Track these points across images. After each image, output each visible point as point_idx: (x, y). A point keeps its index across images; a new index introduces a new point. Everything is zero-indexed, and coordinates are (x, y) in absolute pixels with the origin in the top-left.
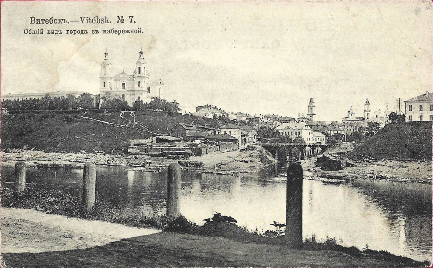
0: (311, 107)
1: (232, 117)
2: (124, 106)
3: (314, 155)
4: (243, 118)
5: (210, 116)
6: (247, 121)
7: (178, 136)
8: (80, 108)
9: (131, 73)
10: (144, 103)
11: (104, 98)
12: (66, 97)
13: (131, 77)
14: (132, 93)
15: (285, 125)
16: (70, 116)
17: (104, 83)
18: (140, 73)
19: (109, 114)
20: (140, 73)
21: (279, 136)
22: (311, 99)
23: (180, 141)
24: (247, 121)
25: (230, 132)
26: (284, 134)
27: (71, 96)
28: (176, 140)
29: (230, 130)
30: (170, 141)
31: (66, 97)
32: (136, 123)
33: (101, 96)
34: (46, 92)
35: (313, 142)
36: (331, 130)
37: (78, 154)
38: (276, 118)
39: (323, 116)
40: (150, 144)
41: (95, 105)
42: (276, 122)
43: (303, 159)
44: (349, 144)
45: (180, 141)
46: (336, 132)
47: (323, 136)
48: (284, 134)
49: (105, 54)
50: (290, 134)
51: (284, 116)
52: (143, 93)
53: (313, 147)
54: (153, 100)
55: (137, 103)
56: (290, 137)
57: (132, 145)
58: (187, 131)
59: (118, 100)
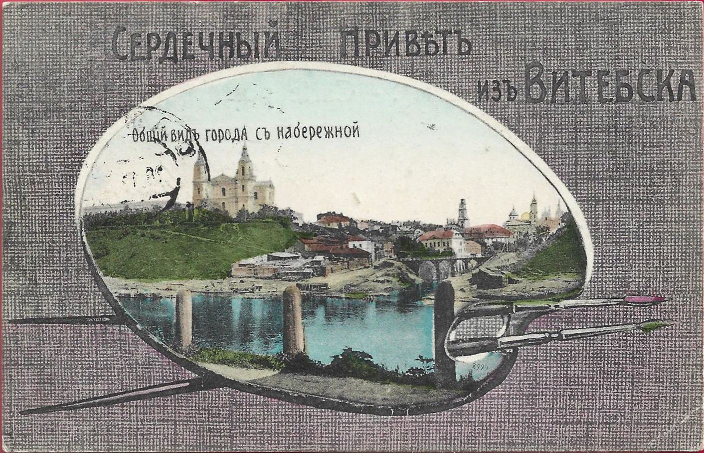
0: (462, 210)
1: (361, 227)
2: (226, 218)
3: (467, 270)
4: (376, 228)
5: (335, 226)
6: (381, 231)
10: (250, 212)
11: (199, 208)
15: (428, 234)
18: (243, 175)
19: (206, 228)
20: (243, 175)
21: (423, 247)
22: (462, 200)
23: (298, 257)
24: (381, 231)
25: (360, 245)
26: (429, 246)
29: (360, 242)
30: (285, 258)
31: (151, 208)
32: (241, 238)
35: (467, 255)
36: (488, 238)
38: (416, 225)
39: (476, 220)
41: (187, 217)
42: (418, 230)
43: (453, 275)
44: (513, 254)
45: (298, 257)
46: (494, 240)
47: (479, 246)
48: (429, 246)
50: (437, 245)
51: (428, 222)
53: (466, 261)
55: (242, 212)
56: (436, 249)
59: (217, 210)
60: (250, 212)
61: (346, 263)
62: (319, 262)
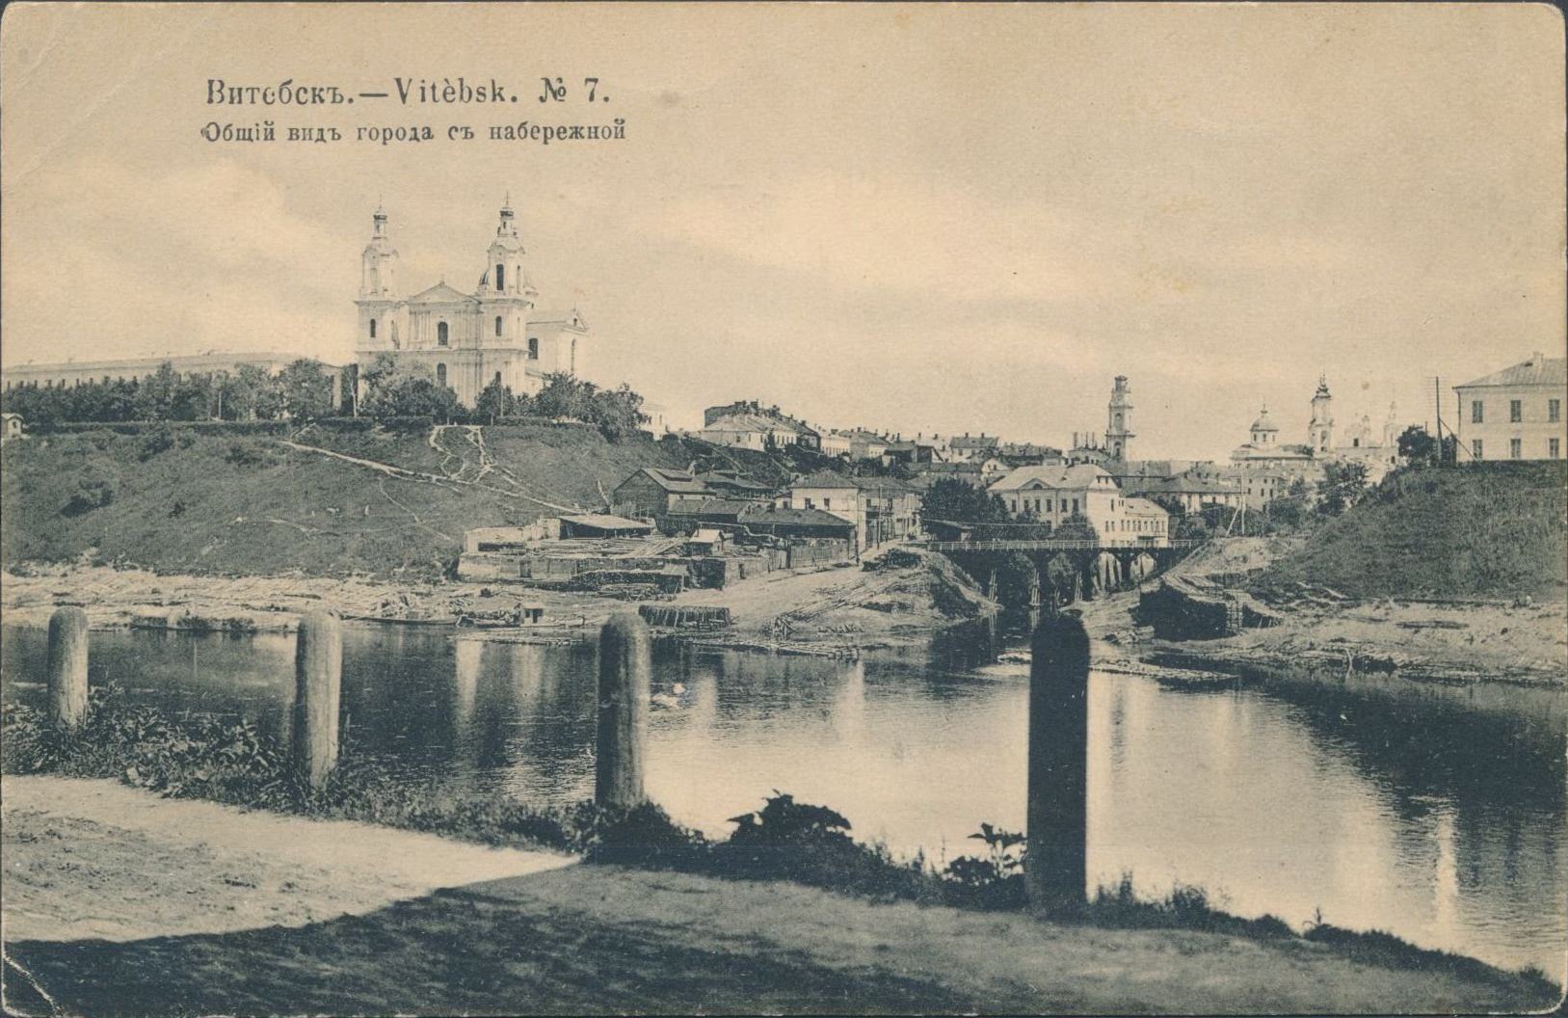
2: (446, 410)
7: (639, 515)
8: (286, 415)
9: (471, 288)
10: (516, 393)
11: (372, 377)
12: (234, 373)
13: (468, 300)
14: (472, 358)
16: (247, 442)
17: (373, 322)
18: (500, 286)
19: (389, 436)
20: (500, 286)
23: (647, 532)
25: (827, 502)
27: (252, 375)
28: (630, 531)
30: (609, 534)
31: (234, 373)
32: (487, 468)
33: (361, 371)
34: (161, 354)
37: (276, 581)
40: (538, 545)
41: (337, 403)
45: (647, 532)
49: (377, 218)
52: (514, 359)
54: (549, 384)
55: (492, 396)
57: (472, 548)
58: (672, 498)
59: (422, 386)
60: (516, 393)
61: (782, 555)
62: (705, 548)
